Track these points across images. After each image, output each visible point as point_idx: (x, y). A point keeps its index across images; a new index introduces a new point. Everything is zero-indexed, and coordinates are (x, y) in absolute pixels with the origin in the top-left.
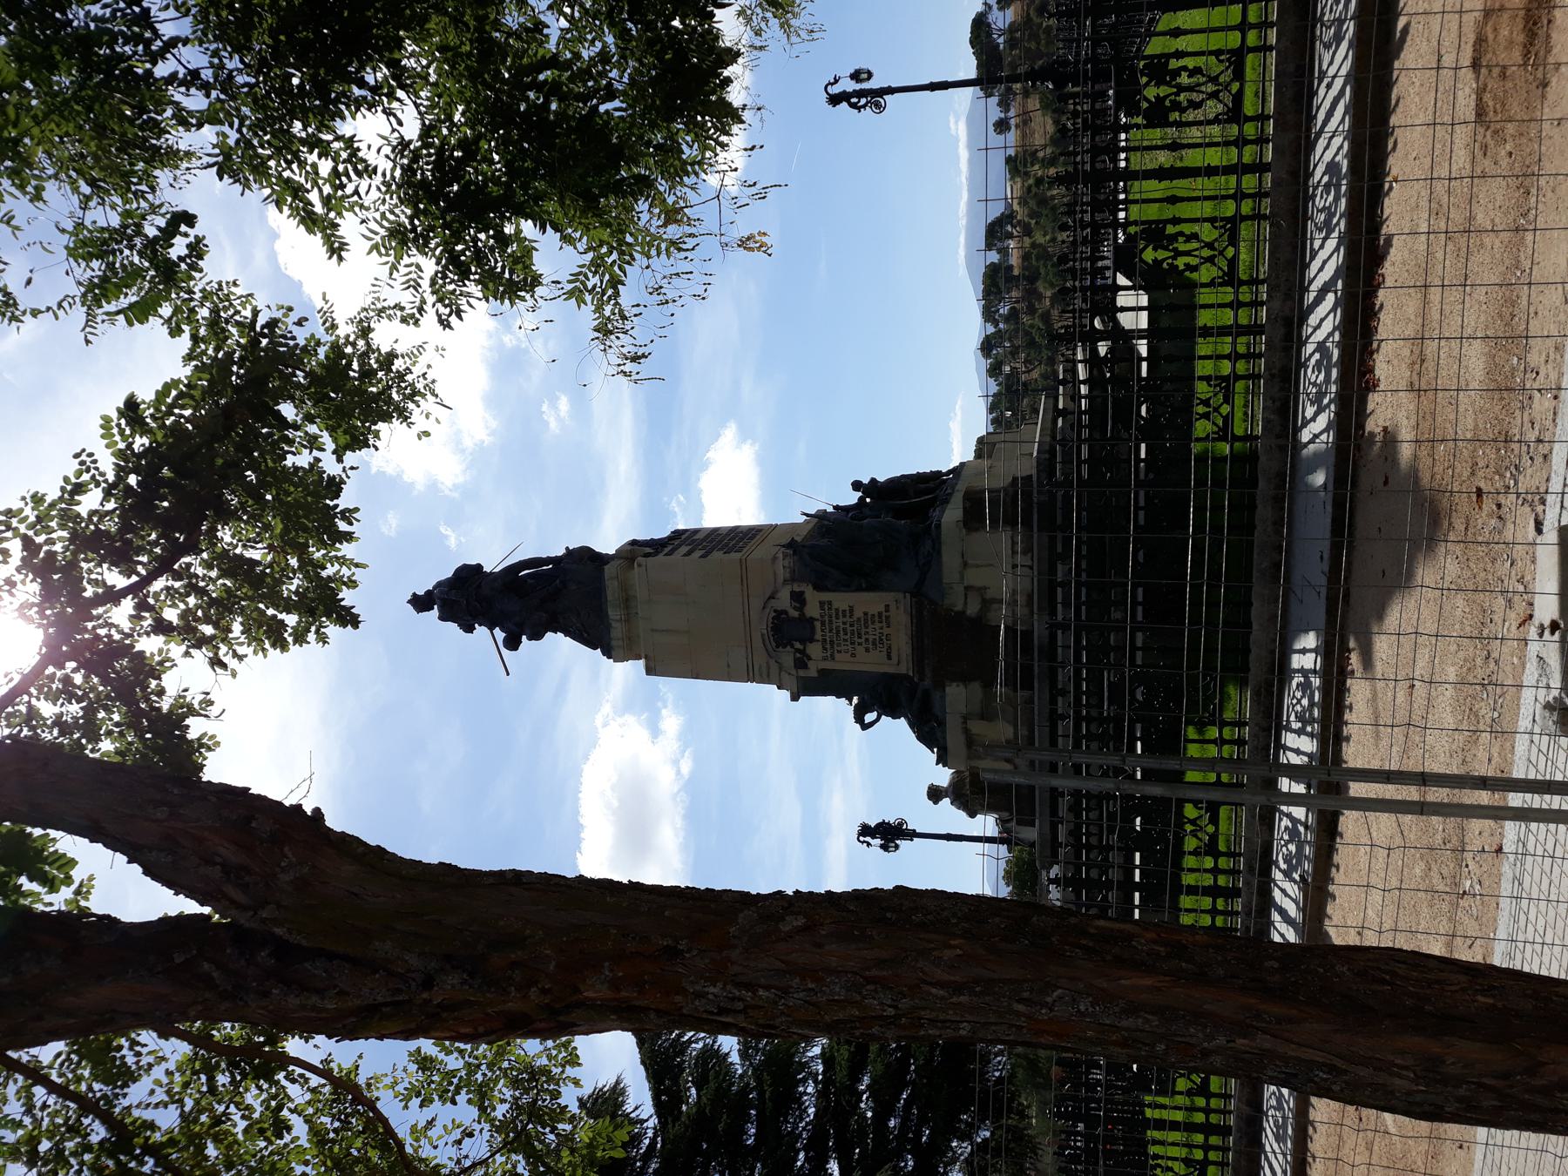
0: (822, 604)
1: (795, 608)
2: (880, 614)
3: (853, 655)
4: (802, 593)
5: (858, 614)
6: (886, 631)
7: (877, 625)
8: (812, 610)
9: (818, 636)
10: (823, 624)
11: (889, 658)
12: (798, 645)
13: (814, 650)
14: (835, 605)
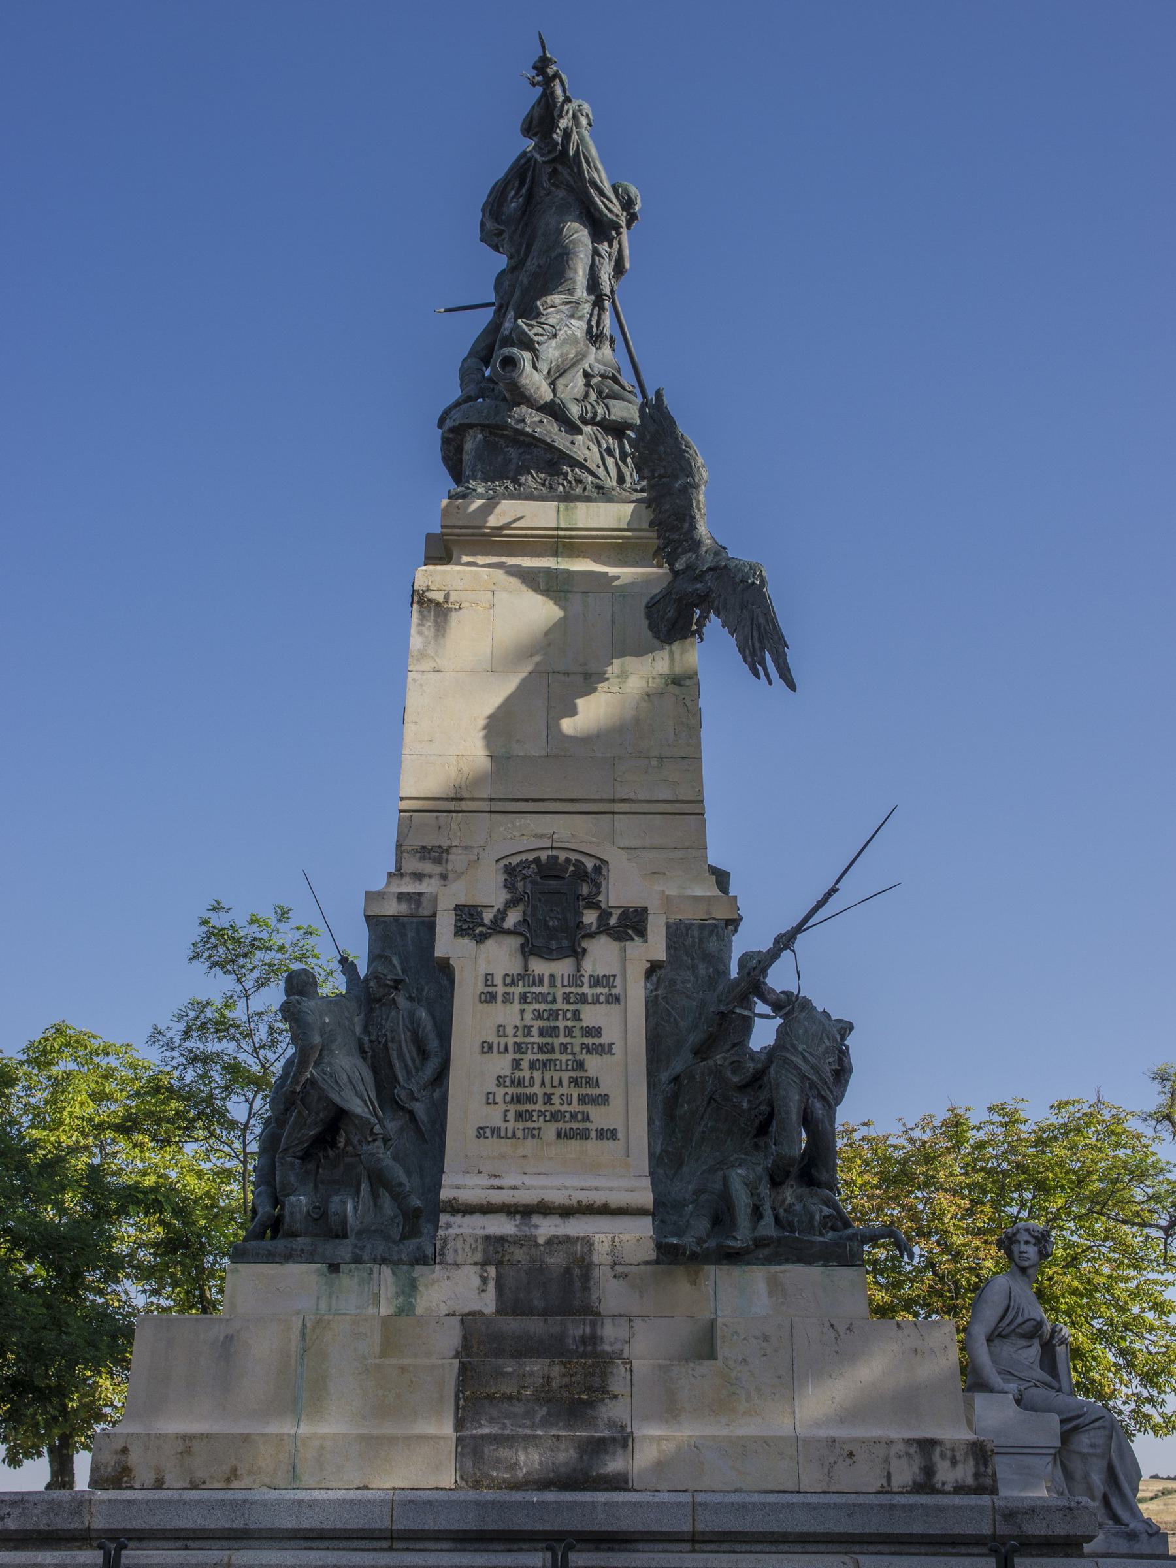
8: (602, 955)
9: (539, 967)
12: (513, 918)
13: (500, 956)
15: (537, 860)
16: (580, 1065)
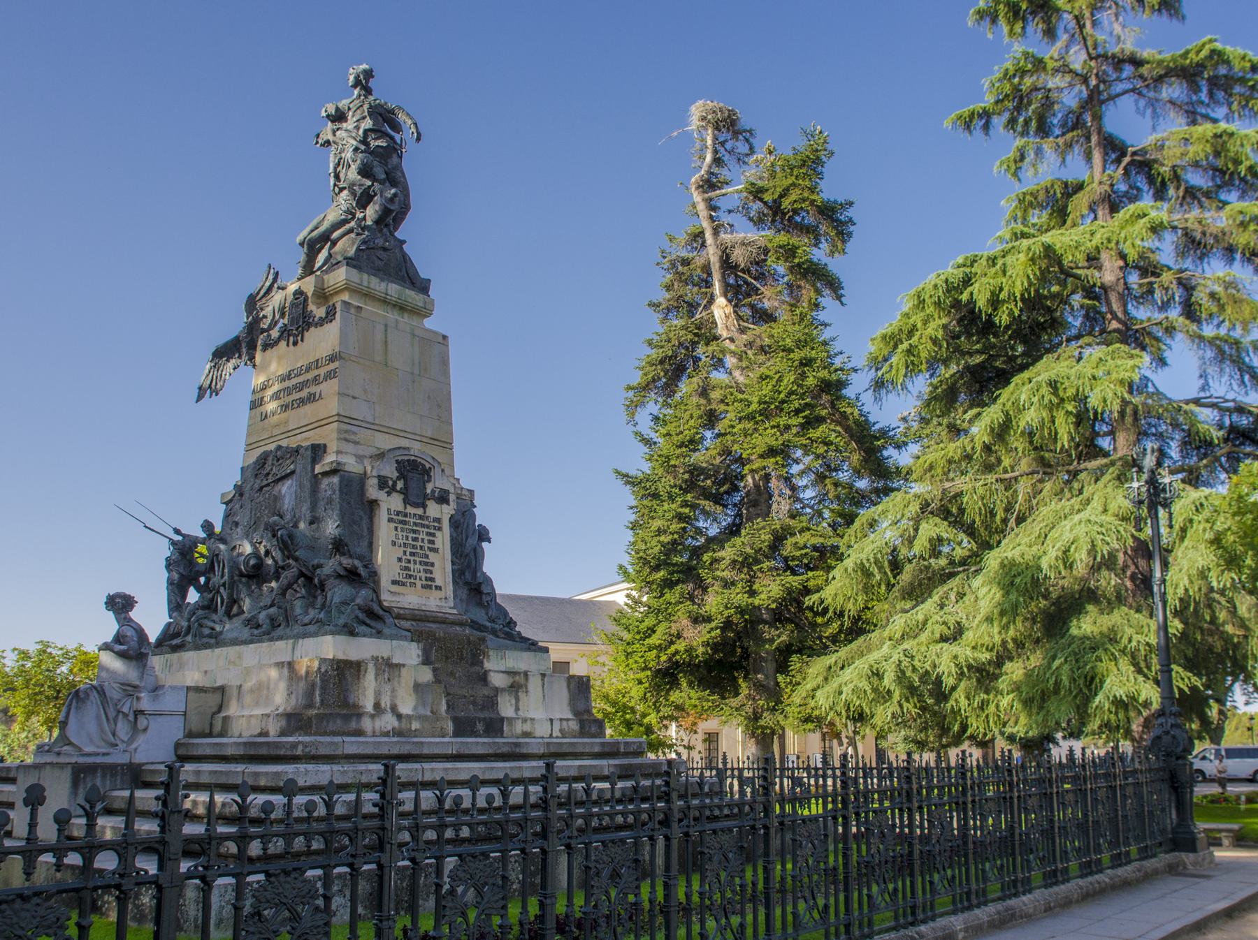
0: (438, 520)
1: (433, 491)
2: (432, 580)
4: (447, 502)
5: (433, 557)
7: (423, 575)
9: (410, 510)
10: (421, 517)
11: (394, 582)
12: (400, 485)
14: (438, 534)
16: (427, 557)
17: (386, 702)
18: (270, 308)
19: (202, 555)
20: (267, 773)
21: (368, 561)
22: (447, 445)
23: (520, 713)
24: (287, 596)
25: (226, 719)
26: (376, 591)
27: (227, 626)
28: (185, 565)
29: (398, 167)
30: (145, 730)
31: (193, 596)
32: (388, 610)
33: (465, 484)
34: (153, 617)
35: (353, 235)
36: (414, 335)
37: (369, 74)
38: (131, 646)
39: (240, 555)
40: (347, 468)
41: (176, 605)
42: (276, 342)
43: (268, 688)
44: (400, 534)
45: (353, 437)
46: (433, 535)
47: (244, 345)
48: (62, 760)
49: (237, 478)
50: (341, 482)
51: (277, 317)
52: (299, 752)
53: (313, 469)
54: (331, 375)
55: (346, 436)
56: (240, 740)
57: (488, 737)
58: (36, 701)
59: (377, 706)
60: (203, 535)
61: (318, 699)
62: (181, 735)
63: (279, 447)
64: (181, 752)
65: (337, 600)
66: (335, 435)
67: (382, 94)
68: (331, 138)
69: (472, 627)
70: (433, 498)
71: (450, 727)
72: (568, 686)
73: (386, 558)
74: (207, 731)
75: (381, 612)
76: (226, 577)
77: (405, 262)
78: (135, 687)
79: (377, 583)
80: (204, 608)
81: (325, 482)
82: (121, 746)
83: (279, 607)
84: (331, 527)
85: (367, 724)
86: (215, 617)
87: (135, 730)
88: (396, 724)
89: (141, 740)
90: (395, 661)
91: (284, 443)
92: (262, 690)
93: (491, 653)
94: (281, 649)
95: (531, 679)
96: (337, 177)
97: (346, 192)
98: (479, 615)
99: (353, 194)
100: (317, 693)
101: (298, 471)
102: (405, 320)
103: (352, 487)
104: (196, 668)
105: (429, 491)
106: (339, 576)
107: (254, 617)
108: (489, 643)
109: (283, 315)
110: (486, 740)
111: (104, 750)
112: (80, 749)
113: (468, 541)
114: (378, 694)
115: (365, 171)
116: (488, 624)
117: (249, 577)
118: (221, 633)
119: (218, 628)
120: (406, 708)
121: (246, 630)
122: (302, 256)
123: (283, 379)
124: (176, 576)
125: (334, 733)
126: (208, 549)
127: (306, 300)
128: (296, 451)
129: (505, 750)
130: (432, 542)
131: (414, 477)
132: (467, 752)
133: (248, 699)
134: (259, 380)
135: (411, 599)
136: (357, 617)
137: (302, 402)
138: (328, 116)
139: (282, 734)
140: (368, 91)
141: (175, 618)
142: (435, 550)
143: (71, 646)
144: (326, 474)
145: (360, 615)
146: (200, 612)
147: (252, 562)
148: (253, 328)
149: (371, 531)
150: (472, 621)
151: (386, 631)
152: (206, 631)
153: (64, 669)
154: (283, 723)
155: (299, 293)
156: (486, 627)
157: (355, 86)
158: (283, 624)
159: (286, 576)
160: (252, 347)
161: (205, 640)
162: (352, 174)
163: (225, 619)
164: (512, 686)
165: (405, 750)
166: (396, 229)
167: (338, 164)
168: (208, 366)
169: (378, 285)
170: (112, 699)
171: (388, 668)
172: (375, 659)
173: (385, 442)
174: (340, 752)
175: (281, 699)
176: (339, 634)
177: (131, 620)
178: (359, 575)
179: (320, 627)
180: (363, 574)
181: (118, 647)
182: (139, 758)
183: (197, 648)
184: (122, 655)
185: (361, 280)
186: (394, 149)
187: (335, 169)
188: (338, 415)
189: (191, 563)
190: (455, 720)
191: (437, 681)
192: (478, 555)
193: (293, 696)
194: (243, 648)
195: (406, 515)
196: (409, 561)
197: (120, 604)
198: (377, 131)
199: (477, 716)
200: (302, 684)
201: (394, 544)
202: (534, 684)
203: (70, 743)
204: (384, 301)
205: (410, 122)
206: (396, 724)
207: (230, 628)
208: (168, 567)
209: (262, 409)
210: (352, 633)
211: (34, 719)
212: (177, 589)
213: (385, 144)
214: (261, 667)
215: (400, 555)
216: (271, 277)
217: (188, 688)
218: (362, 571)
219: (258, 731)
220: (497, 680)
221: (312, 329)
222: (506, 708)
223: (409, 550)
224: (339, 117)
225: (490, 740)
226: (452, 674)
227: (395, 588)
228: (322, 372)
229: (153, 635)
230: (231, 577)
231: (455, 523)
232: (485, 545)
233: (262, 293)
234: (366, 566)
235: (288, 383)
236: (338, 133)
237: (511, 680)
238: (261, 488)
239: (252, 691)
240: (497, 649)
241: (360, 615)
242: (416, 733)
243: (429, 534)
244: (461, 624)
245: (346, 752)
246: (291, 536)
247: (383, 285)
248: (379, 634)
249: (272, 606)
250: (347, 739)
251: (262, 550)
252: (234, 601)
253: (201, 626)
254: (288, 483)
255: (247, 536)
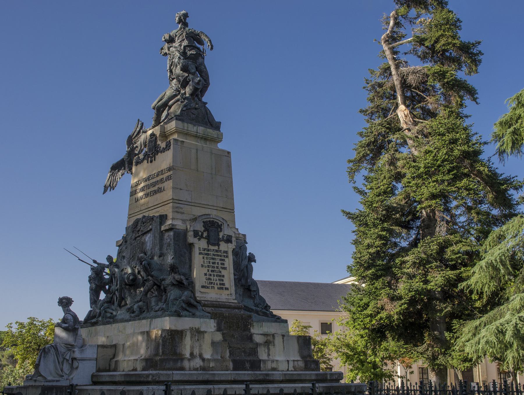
0: (226, 252)
2: (223, 284)
3: (202, 266)
4: (231, 242)
5: (224, 272)
6: (216, 287)
7: (218, 282)
9: (211, 247)
10: (217, 251)
11: (203, 287)
12: (205, 234)
13: (203, 244)
14: (226, 259)
15: (210, 221)
16: (220, 272)
17: (196, 352)
18: (139, 143)
19: (107, 274)
20: (133, 390)
21: (189, 276)
22: (232, 211)
23: (271, 357)
24: (148, 296)
25: (117, 362)
26: (193, 292)
27: (119, 312)
28: (98, 280)
29: (203, 64)
30: (77, 368)
31: (102, 296)
32: (199, 302)
33: (241, 231)
34: (82, 309)
35: (179, 103)
36: (212, 153)
37: (186, 16)
38: (71, 324)
39: (125, 274)
40: (177, 227)
41: (94, 300)
42: (142, 161)
43: (137, 345)
44: (206, 260)
45: (180, 210)
46: (223, 260)
47: (126, 163)
48: (37, 384)
49: (124, 233)
50: (174, 234)
51: (143, 147)
52: (150, 379)
53: (161, 228)
54: (169, 178)
55: (177, 210)
56: (124, 373)
57: (252, 371)
58: (28, 351)
59: (192, 354)
60: (107, 263)
61: (161, 351)
62: (94, 371)
63: (144, 217)
64: (95, 380)
65: (172, 298)
66: (171, 210)
67: (194, 26)
68: (167, 51)
69: (245, 310)
70: (223, 240)
71: (231, 365)
72: (298, 342)
73: (198, 274)
74: (108, 368)
75: (195, 303)
76: (118, 286)
77: (207, 114)
78: (72, 345)
79: (193, 287)
80: (107, 302)
81: (167, 234)
82: (65, 377)
83: (144, 302)
84: (170, 259)
85: (186, 364)
86: (113, 307)
87: (72, 368)
88: (202, 364)
89: (75, 373)
90: (202, 330)
91: (146, 214)
92: (135, 347)
93: (255, 324)
94: (143, 324)
95: (276, 338)
96: (171, 71)
97: (175, 80)
98: (249, 303)
99: (179, 81)
100: (161, 347)
101: (153, 229)
102: (208, 146)
103: (180, 237)
104: (103, 335)
105: (221, 237)
106: (173, 285)
107: (131, 307)
108: (254, 318)
109: (145, 146)
110: (250, 372)
111: (57, 379)
112: (45, 378)
113: (243, 263)
114: (192, 348)
115: (184, 69)
116: (254, 308)
117: (130, 285)
118: (116, 316)
119: (114, 313)
120: (207, 355)
121: (128, 314)
122: (153, 114)
123: (146, 180)
124: (94, 286)
125: (169, 369)
126: (110, 270)
127: (156, 139)
128: (152, 219)
129: (261, 377)
130: (223, 264)
131: (213, 230)
132: (239, 379)
133: (128, 352)
134: (134, 181)
135: (212, 295)
136: (182, 307)
137: (155, 192)
138: (165, 41)
139: (144, 370)
140: (185, 25)
141: (93, 308)
142: (225, 268)
143: (46, 320)
144: (167, 231)
145: (184, 305)
146: (106, 305)
147: (131, 278)
148: (131, 154)
149: (190, 260)
150: (245, 306)
151: (198, 313)
152: (109, 315)
153: (42, 333)
154: (144, 364)
155: (153, 135)
156: (252, 310)
157: (179, 23)
158: (146, 311)
159: (148, 284)
160: (130, 164)
161: (108, 320)
162: (178, 71)
163: (118, 308)
164: (266, 342)
165: (206, 378)
166: (202, 96)
167: (171, 65)
168: (109, 175)
169: (192, 128)
170: (61, 352)
171: (198, 333)
172: (191, 329)
173: (198, 212)
174: (171, 379)
175: (143, 352)
176: (172, 316)
177: (70, 310)
178: (183, 284)
179: (163, 312)
180: (185, 283)
181: (64, 325)
182: (74, 382)
183: (104, 324)
184: (66, 329)
185: (184, 126)
186: (200, 54)
187: (170, 67)
188: (173, 199)
189: (101, 278)
190: (234, 361)
191: (225, 340)
192: (249, 270)
193: (149, 349)
194: (126, 324)
195: (208, 250)
196: (211, 275)
197: (65, 303)
198: (191, 46)
199: (245, 357)
200: (153, 343)
201: (202, 266)
202: (278, 340)
203: (41, 375)
204: (196, 136)
205: (207, 40)
206: (202, 364)
207: (121, 313)
208: (90, 281)
209: (136, 196)
210: (179, 316)
211: (27, 361)
212: (94, 293)
213: (195, 53)
214: (134, 334)
215: (206, 272)
216: (139, 126)
217: (98, 346)
218: (185, 282)
219: (132, 368)
220: (258, 339)
221: (159, 154)
222: (263, 355)
223: (210, 269)
224: (171, 40)
225: (252, 372)
226: (233, 336)
227: (203, 290)
228: (165, 176)
229: (82, 317)
230: (121, 286)
231: (235, 253)
232: (253, 263)
233: (135, 134)
234: (187, 279)
235: (147, 183)
236: (171, 49)
237: (266, 339)
238: (136, 238)
239: (129, 347)
240: (258, 322)
241: (184, 305)
242: (213, 369)
243: (221, 260)
244: (239, 308)
245: (174, 379)
246: (149, 264)
247: (195, 128)
248: (194, 315)
249: (140, 301)
250: (175, 372)
251: (136, 271)
252: (122, 299)
253: (106, 312)
254: (149, 235)
255: (129, 263)
